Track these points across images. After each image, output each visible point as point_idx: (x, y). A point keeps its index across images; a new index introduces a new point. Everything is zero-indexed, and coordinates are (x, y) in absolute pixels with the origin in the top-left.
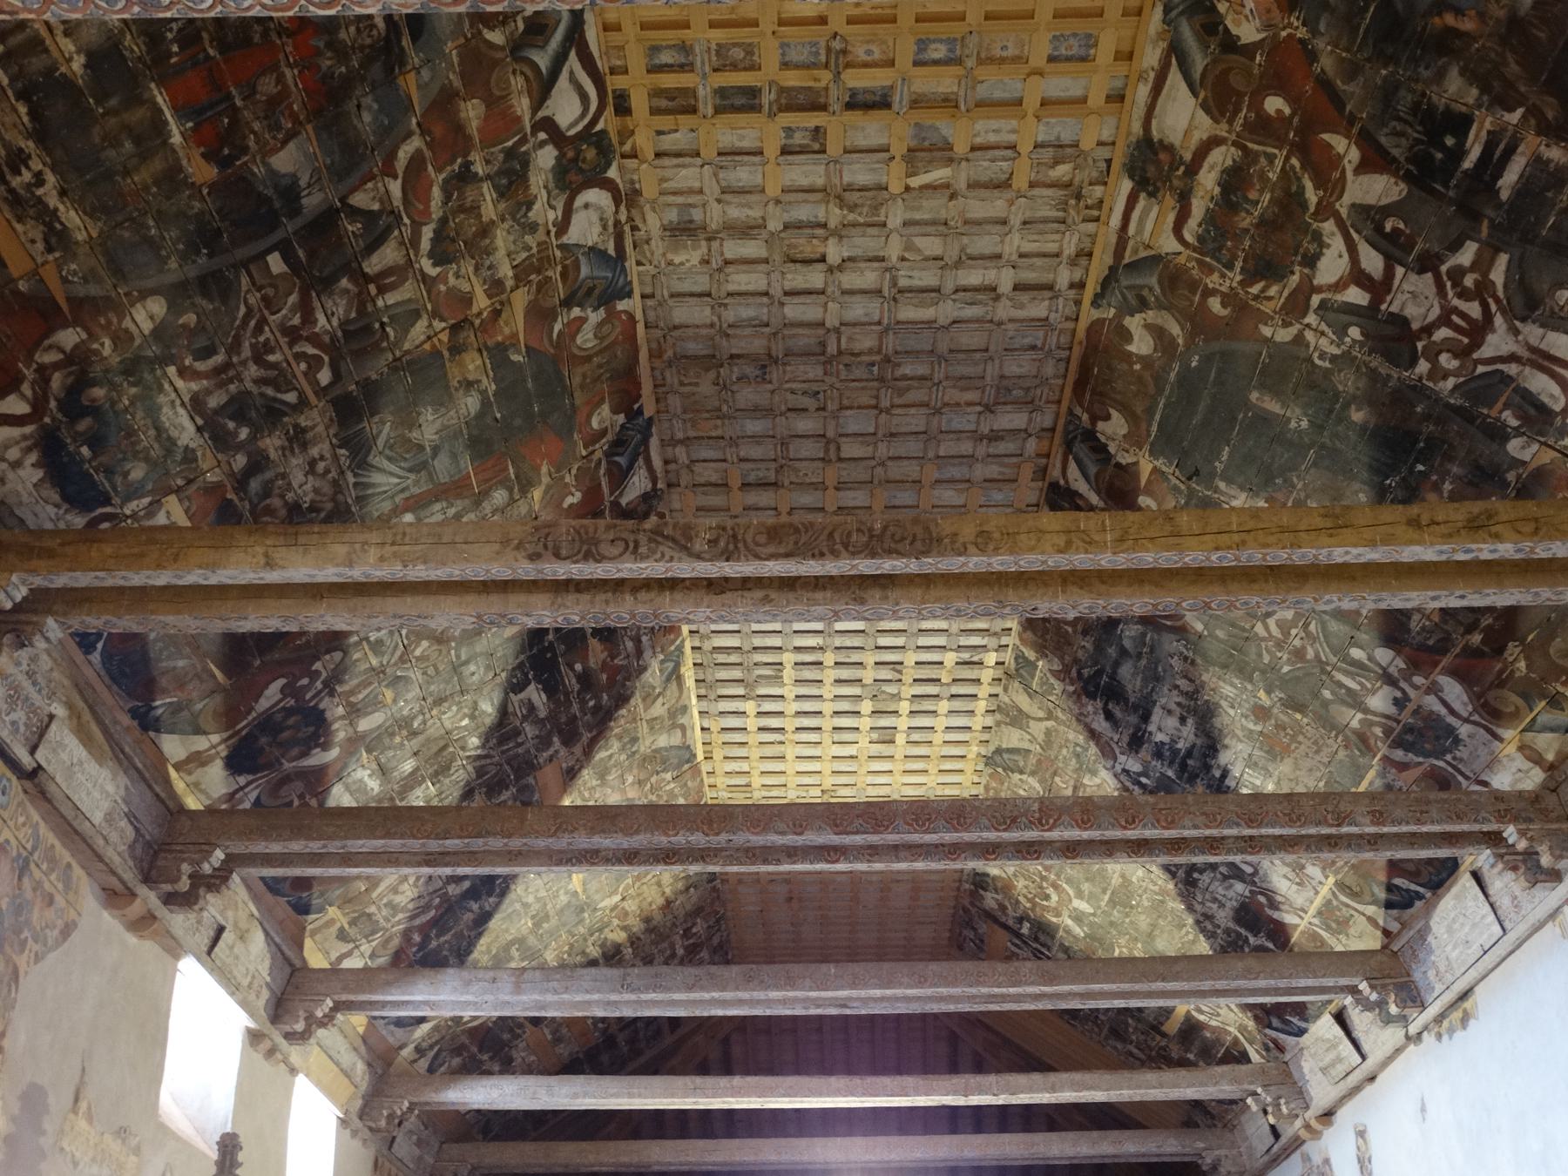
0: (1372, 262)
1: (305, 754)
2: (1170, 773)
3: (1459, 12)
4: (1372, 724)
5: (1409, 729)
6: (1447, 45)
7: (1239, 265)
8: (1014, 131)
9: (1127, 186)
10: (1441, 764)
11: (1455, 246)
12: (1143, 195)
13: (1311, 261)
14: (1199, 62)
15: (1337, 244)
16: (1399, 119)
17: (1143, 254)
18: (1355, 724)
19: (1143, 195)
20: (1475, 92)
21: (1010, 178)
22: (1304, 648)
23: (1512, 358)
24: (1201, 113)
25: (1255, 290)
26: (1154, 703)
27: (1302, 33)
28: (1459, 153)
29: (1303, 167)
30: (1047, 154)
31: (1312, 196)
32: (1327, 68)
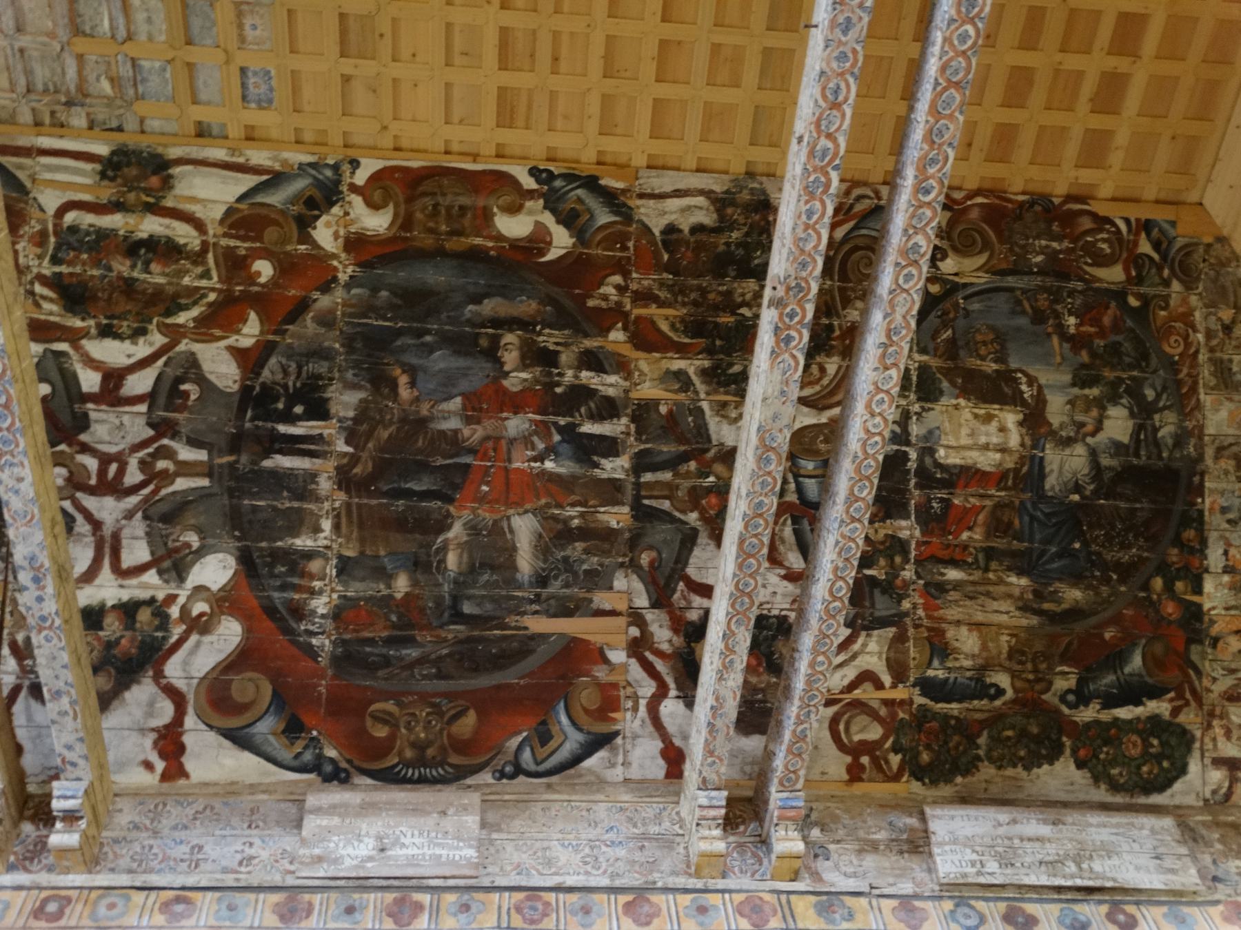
0: (140, 383)
3: (412, 384)
6: (381, 383)
7: (64, 269)
8: (150, 38)
9: (103, 150)
11: (194, 443)
12: (98, 167)
13: (106, 332)
14: (276, 198)
15: (142, 350)
16: (300, 367)
17: (21, 175)
19: (98, 167)
20: (351, 414)
21: (85, 35)
23: (96, 525)
24: (223, 208)
25: (38, 288)
27: (343, 277)
28: (291, 419)
29: (210, 305)
30: (126, 71)
31: (182, 318)
32: (318, 305)
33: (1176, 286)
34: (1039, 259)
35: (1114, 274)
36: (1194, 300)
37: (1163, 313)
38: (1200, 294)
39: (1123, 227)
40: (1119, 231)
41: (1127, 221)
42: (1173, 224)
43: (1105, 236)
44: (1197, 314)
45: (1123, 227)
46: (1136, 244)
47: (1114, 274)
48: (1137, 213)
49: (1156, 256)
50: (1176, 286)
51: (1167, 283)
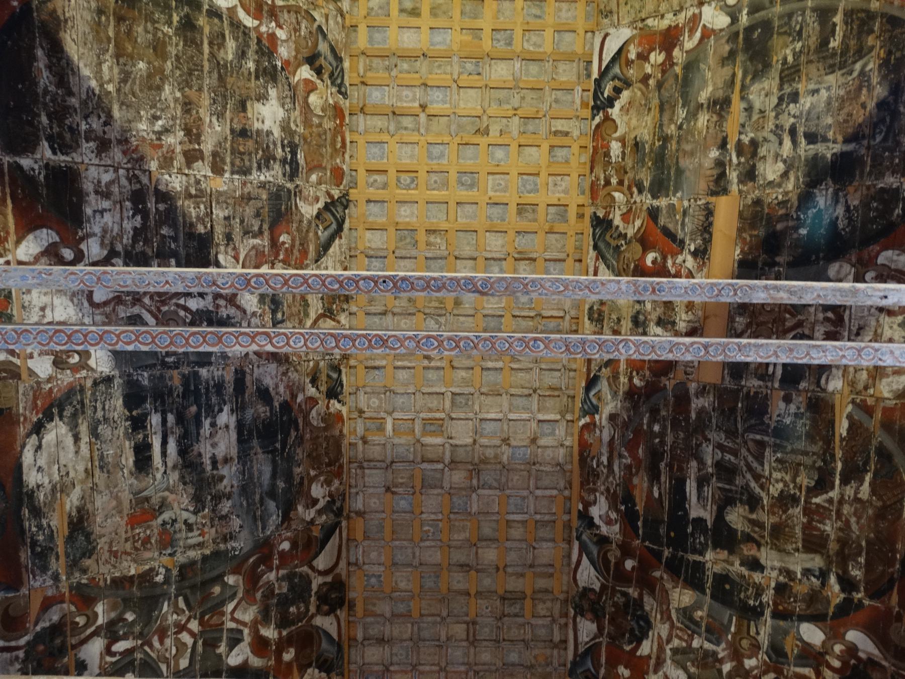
1: (871, 662)
2: (204, 372)
4: (87, 626)
5: (62, 651)
10: (23, 641)
18: (99, 608)
22: (162, 642)
26: (239, 457)
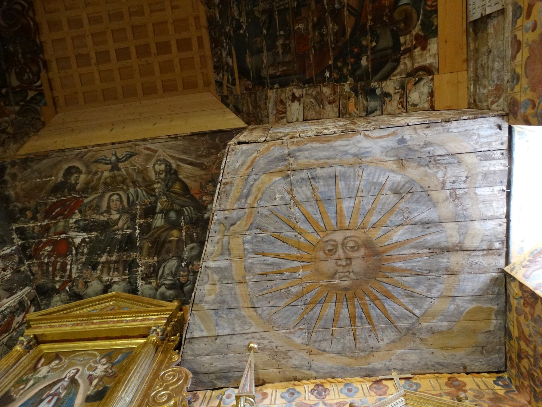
33: (17, 108)
34: (11, 49)
35: (15, 82)
36: (14, 116)
37: (2, 104)
38: (16, 119)
39: (38, 84)
40: (36, 82)
41: (41, 86)
42: (45, 104)
43: (31, 77)
44: (7, 118)
45: (38, 84)
46: (31, 90)
47: (15, 82)
48: (46, 88)
49: (28, 98)
50: (17, 108)
51: (17, 104)
